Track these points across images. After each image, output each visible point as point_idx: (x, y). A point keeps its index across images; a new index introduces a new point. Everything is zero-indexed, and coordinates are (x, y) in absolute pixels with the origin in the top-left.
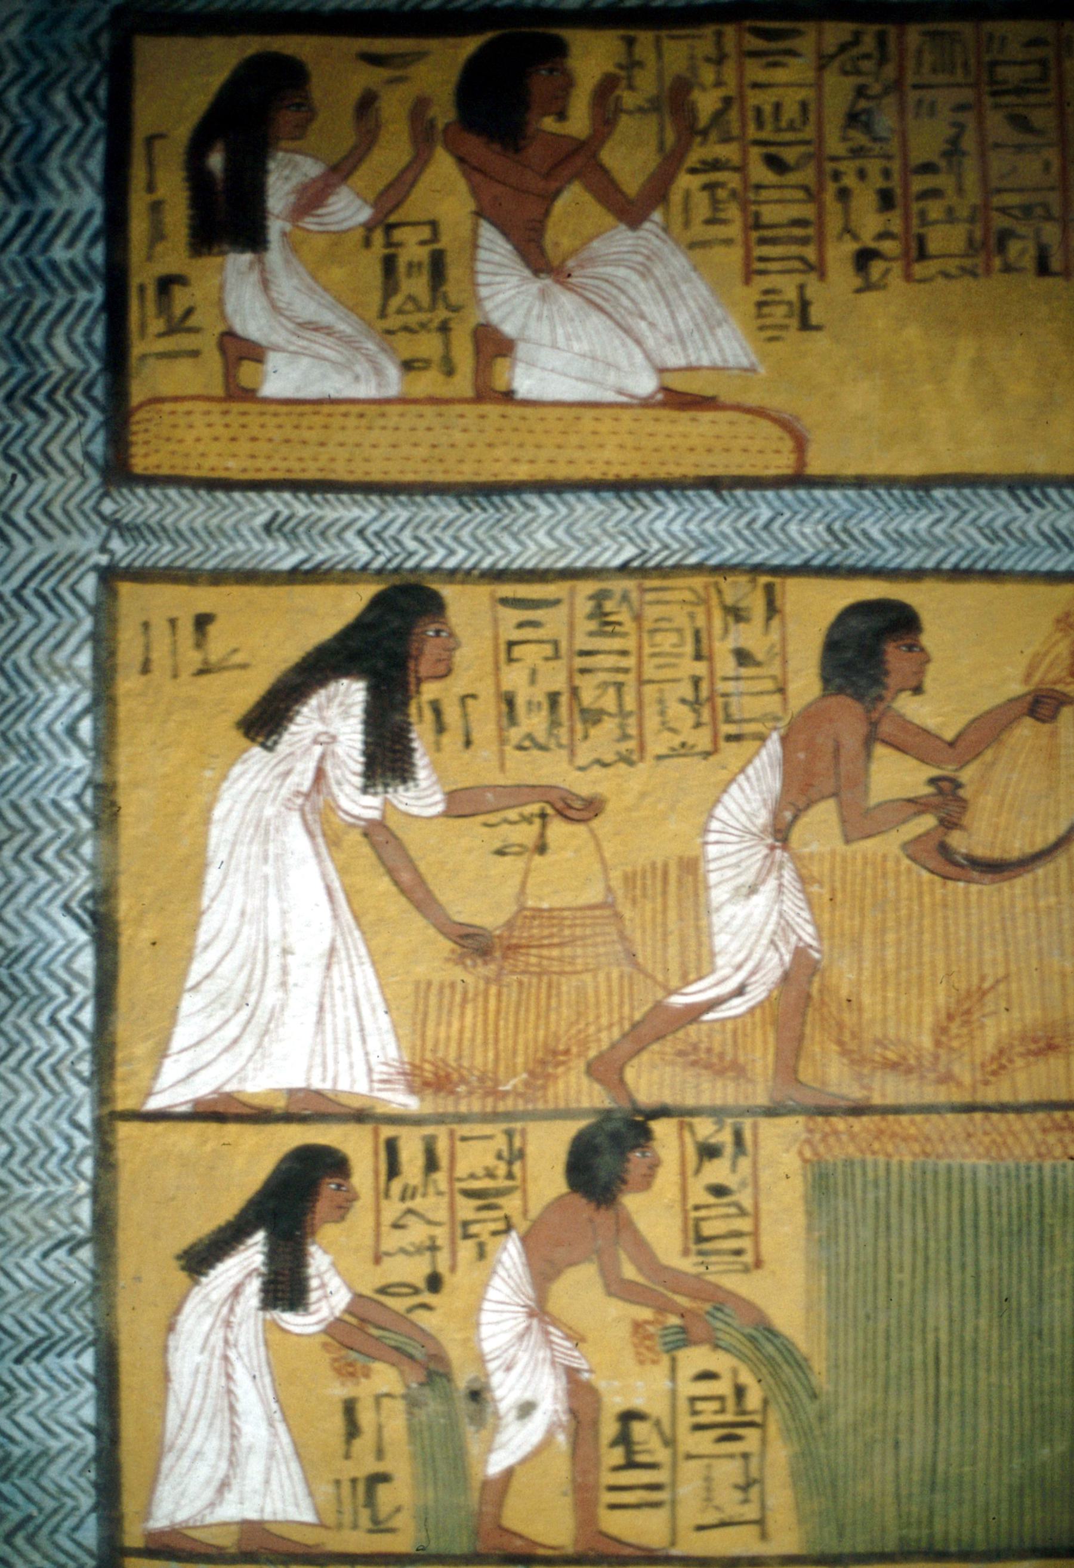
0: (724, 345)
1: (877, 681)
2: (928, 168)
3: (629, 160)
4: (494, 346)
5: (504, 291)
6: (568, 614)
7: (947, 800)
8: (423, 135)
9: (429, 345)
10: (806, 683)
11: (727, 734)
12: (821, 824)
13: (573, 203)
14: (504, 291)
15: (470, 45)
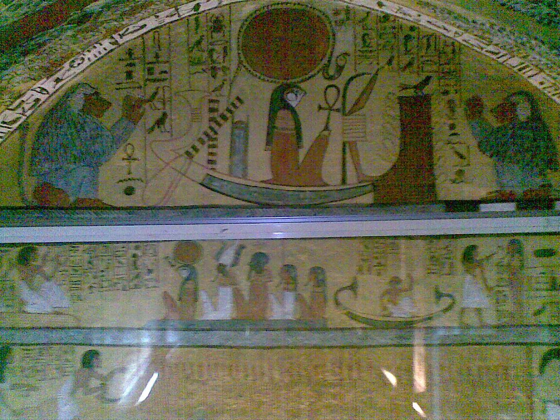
0: (65, 303)
1: (92, 366)
2: (102, 271)
3: (48, 269)
4: (23, 302)
5: (25, 292)
6: (35, 352)
7: (103, 387)
8: (12, 266)
9: (10, 303)
10: (79, 365)
11: (63, 373)
12: (80, 393)
13: (38, 279)
14: (25, 292)
15: (18, 249)
